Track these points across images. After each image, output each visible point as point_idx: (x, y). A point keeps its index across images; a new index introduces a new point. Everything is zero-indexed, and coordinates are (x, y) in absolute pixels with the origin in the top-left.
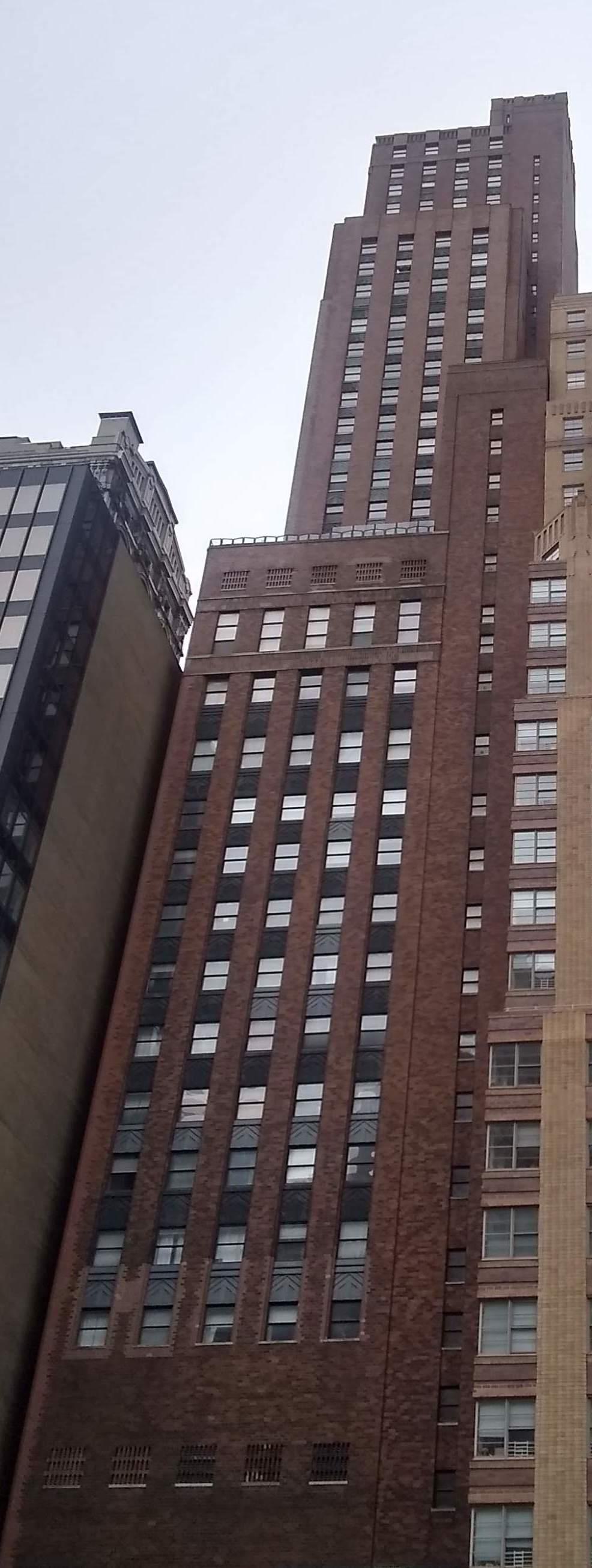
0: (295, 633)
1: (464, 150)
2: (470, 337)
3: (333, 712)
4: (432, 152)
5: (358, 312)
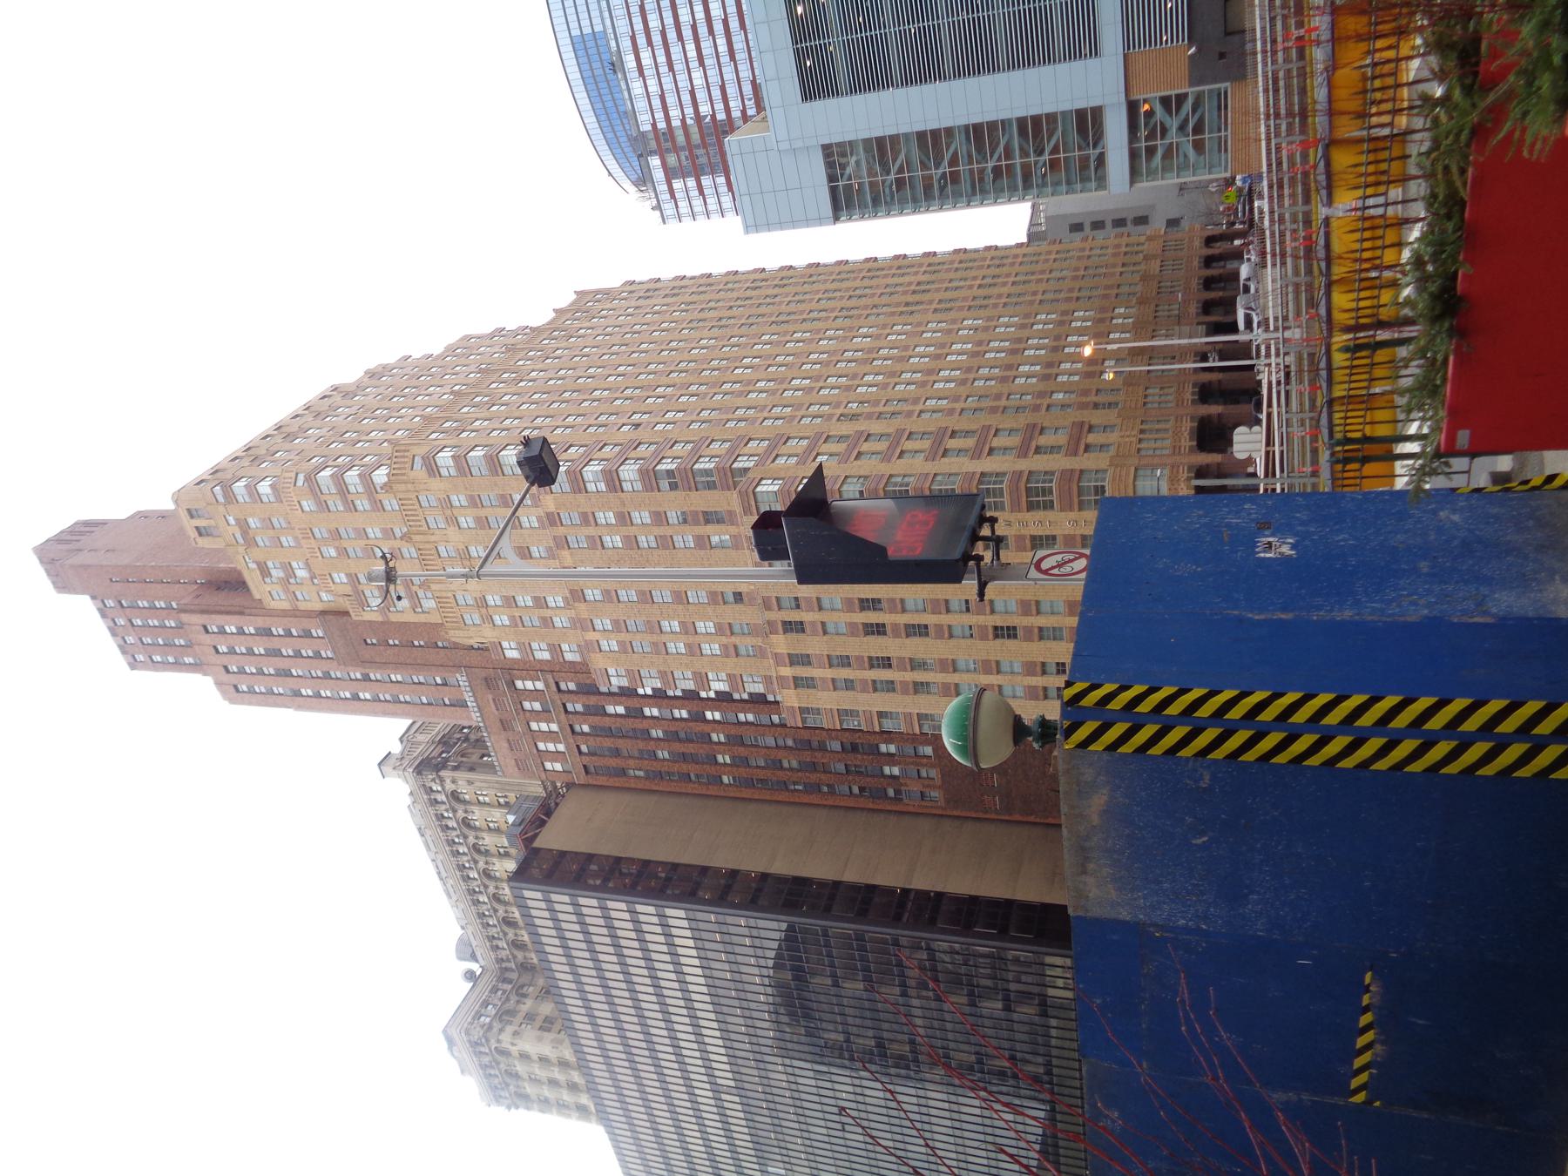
0: (550, 736)
1: (121, 622)
2: (294, 632)
3: (596, 720)
4: (130, 639)
5: (297, 694)
